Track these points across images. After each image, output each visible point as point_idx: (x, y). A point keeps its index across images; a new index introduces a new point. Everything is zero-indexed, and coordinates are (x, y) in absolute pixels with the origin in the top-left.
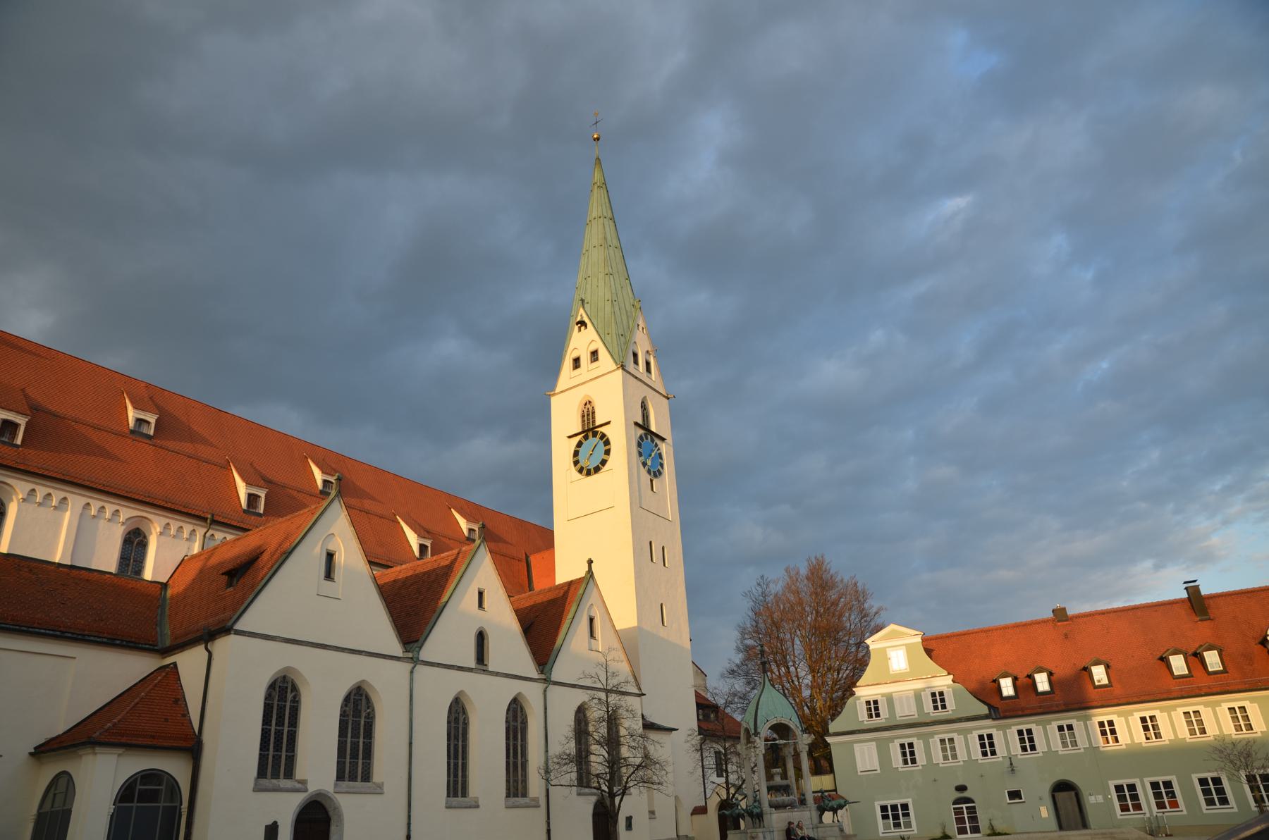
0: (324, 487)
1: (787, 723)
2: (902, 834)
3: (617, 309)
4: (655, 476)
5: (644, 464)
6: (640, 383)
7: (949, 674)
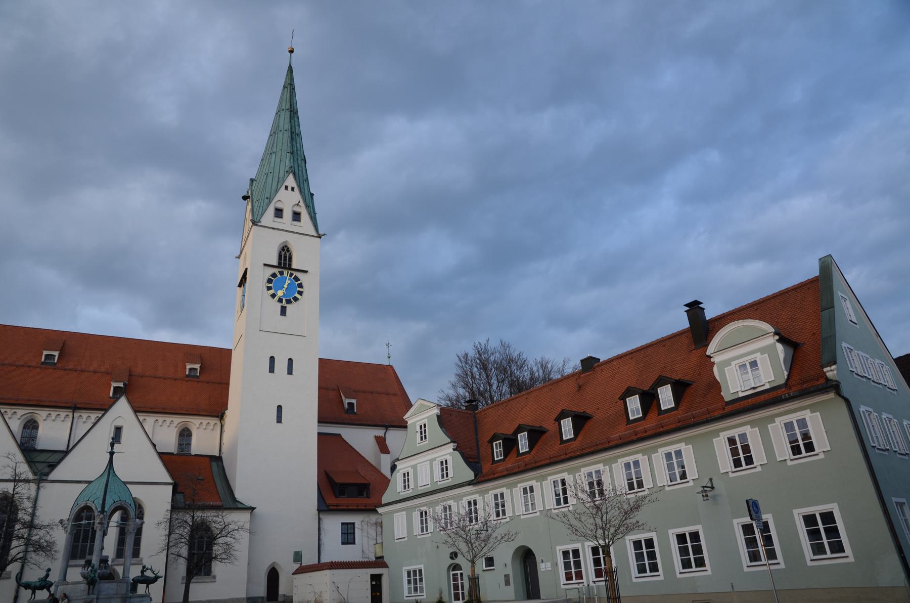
0: (46, 359)
1: (90, 505)
2: (417, 598)
3: (270, 179)
4: (289, 302)
5: (273, 296)
7: (452, 442)
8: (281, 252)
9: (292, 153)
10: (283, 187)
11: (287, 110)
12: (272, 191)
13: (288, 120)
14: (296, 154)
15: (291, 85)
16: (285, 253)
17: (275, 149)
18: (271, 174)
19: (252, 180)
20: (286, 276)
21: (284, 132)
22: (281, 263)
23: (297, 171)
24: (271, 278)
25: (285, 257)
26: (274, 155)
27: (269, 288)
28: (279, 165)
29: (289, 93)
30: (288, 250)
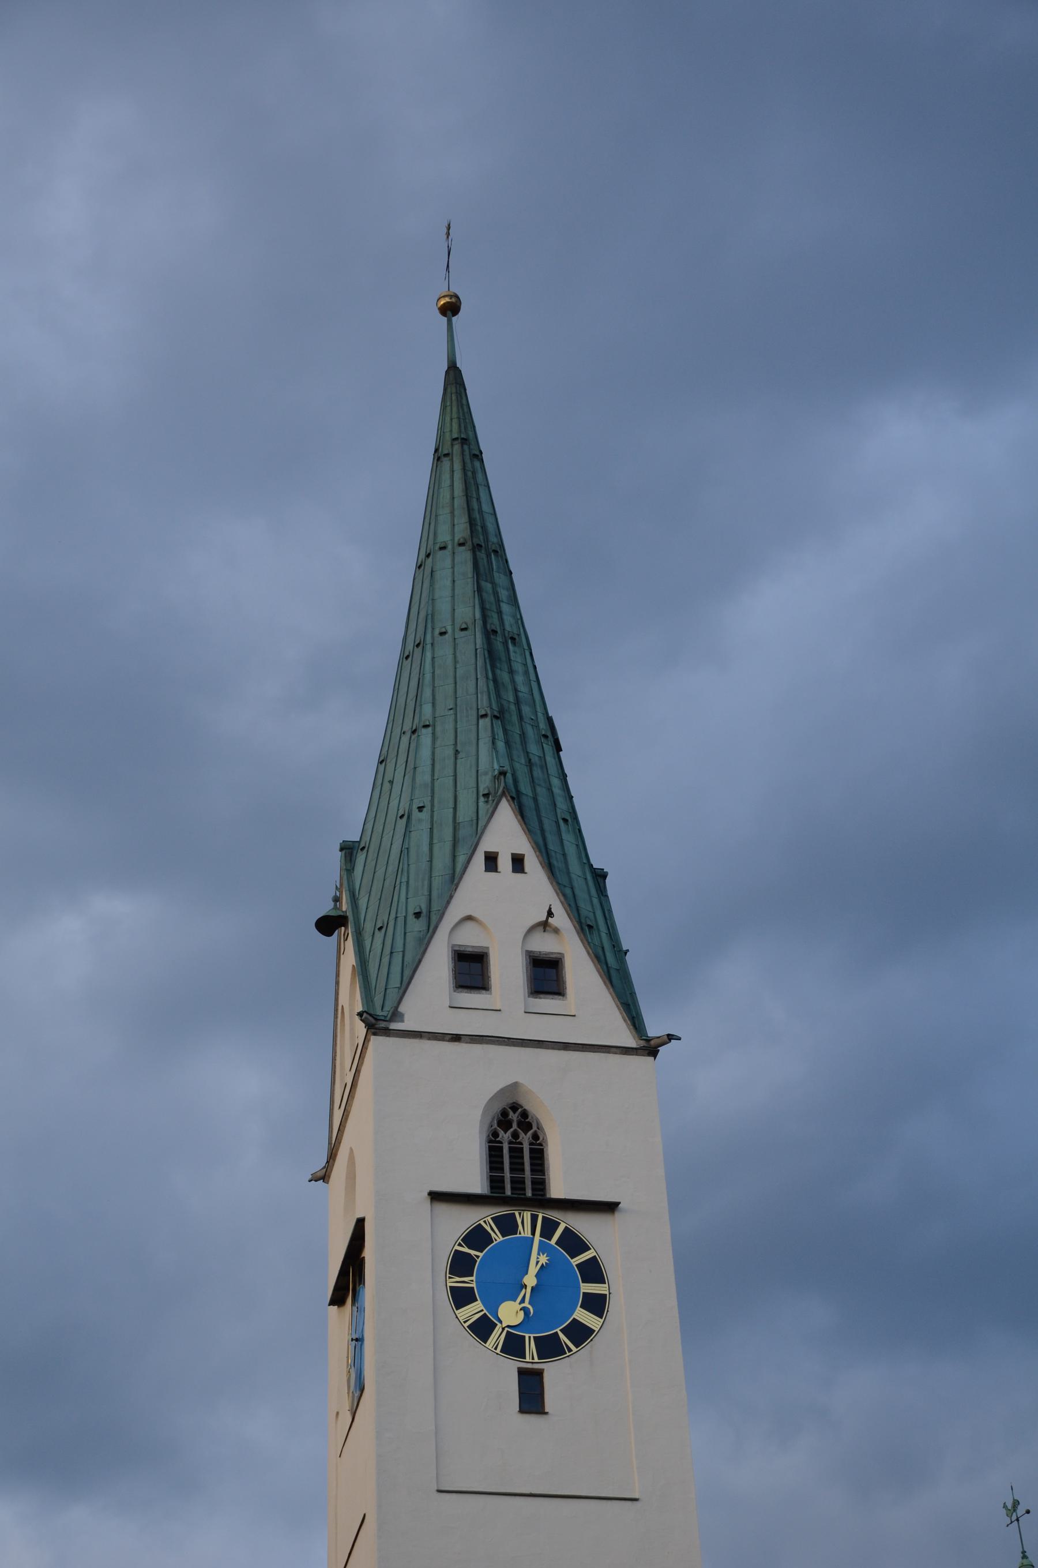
3: (420, 836)
4: (550, 1348)
5: (482, 1328)
6: (477, 1049)
8: (495, 1134)
9: (499, 716)
10: (479, 860)
11: (461, 545)
12: (436, 883)
13: (466, 586)
14: (515, 718)
15: (464, 441)
16: (515, 1135)
17: (427, 709)
18: (425, 815)
19: (349, 850)
20: (527, 1233)
21: (459, 634)
22: (502, 1180)
23: (525, 788)
24: (466, 1250)
25: (516, 1152)
26: (426, 735)
27: (461, 1297)
28: (450, 771)
29: (458, 475)
30: (526, 1122)
